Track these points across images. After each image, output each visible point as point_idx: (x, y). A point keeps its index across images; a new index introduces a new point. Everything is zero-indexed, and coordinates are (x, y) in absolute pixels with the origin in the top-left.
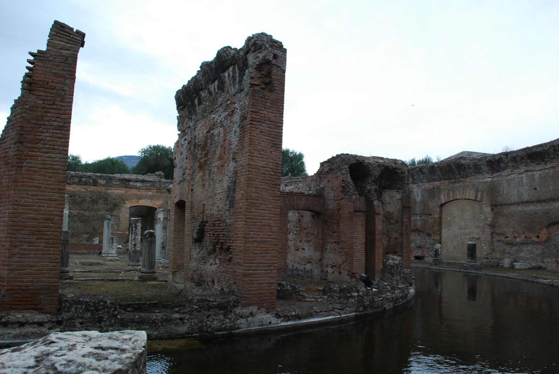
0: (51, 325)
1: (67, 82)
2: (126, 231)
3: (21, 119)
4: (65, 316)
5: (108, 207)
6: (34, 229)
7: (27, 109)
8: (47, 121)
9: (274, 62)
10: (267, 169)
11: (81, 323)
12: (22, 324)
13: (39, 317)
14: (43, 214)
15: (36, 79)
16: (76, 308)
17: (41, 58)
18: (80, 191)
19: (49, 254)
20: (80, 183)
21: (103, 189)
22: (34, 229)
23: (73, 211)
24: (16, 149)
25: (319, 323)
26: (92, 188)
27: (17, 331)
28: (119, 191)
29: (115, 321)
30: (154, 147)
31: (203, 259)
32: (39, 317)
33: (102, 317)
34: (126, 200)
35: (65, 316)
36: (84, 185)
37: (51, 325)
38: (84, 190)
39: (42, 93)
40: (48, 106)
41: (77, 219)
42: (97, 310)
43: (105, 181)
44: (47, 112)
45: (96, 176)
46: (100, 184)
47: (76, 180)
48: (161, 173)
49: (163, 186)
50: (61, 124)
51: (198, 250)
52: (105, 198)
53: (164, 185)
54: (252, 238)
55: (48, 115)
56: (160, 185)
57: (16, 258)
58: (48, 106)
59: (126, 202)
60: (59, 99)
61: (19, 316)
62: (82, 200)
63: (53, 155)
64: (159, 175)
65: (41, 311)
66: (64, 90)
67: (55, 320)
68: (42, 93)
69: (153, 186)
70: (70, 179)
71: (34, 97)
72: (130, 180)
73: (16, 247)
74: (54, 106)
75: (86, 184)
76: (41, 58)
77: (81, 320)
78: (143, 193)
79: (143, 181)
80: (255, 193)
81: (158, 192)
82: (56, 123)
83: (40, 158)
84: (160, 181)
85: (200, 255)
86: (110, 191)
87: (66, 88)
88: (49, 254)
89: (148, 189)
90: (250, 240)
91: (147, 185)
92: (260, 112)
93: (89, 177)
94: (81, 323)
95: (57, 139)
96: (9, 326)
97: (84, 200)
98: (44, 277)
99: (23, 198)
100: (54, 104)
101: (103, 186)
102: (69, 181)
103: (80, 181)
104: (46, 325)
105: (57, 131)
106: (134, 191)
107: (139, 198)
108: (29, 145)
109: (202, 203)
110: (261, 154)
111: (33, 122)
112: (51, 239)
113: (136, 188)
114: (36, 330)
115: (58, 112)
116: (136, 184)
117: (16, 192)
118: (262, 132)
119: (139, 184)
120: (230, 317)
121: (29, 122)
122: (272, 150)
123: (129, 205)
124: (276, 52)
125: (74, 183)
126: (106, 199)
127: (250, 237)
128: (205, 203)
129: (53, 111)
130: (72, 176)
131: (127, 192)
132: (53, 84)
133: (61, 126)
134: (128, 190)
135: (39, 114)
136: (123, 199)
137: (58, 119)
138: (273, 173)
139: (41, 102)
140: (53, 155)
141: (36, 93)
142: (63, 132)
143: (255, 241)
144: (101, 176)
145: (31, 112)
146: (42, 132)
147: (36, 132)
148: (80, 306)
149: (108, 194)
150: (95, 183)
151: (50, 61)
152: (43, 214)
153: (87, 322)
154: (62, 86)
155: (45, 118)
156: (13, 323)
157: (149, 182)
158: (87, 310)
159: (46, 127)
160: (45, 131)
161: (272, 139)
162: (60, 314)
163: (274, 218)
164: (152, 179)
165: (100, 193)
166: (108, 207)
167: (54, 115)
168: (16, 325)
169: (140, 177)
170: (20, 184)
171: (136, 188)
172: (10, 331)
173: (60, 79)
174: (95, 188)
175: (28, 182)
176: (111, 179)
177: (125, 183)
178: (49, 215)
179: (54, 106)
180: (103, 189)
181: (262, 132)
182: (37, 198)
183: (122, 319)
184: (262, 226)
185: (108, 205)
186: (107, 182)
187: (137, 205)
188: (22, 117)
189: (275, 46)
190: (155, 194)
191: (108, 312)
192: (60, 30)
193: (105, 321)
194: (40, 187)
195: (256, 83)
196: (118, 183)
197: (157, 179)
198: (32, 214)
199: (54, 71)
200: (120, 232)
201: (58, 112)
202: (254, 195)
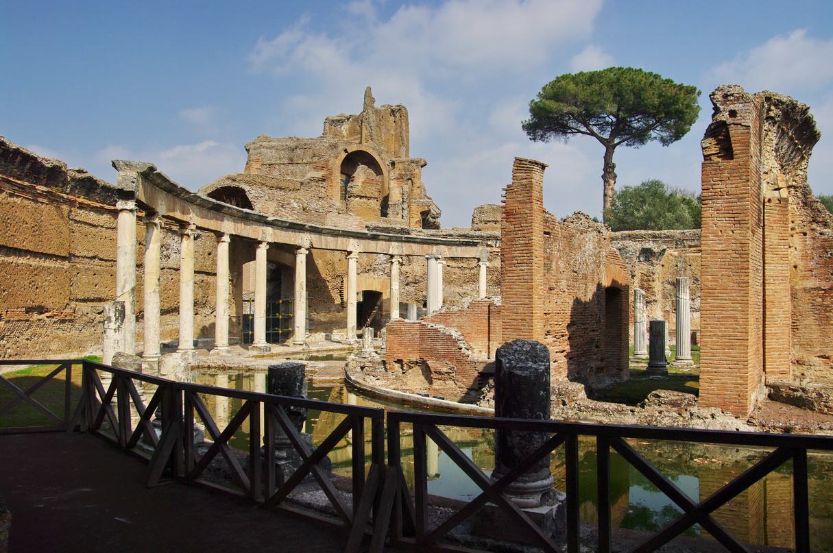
1: (528, 206)
9: (730, 120)
10: (728, 252)
15: (508, 209)
39: (512, 220)
40: (517, 229)
54: (710, 332)
55: (517, 236)
66: (526, 214)
68: (512, 220)
80: (711, 281)
87: (527, 211)
90: (709, 334)
92: (714, 187)
110: (718, 236)
115: (523, 232)
118: (718, 210)
120: (684, 415)
122: (734, 229)
124: (732, 107)
127: (707, 331)
135: (512, 236)
138: (738, 256)
143: (715, 335)
146: (515, 251)
154: (524, 210)
160: (517, 249)
161: (733, 216)
163: (740, 308)
181: (718, 210)
184: (722, 317)
189: (731, 101)
191: (568, 397)
192: (518, 167)
195: (714, 152)
202: (709, 284)
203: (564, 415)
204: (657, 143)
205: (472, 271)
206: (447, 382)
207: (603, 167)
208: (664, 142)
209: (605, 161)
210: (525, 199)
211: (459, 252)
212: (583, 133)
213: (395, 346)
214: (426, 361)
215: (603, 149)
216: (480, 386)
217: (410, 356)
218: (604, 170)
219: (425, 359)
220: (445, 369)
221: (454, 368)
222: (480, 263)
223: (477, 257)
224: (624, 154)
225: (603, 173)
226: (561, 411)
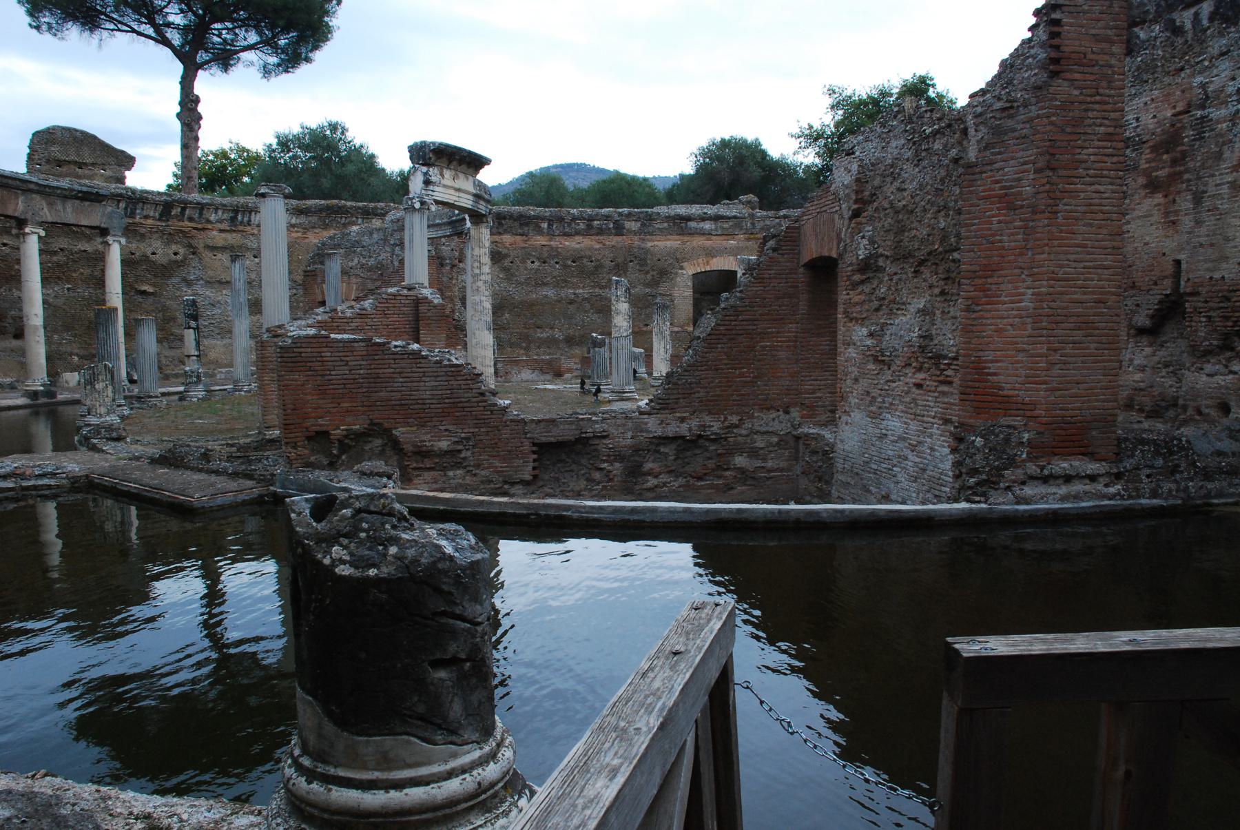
0: (1107, 480)
2: (688, 325)
3: (1049, 128)
4: (1128, 464)
5: (649, 277)
6: (1081, 319)
7: (1057, 107)
8: (1090, 126)
11: (1148, 476)
12: (1068, 479)
13: (1092, 467)
14: (1093, 293)
16: (1142, 451)
17: (1072, 9)
18: (591, 249)
19: (1103, 361)
20: (589, 231)
21: (636, 241)
22: (1081, 319)
23: (581, 291)
24: (1045, 180)
25: (1031, 516)
26: (614, 240)
27: (1063, 490)
28: (668, 243)
29: (1196, 473)
30: (723, 141)
31: (1166, 366)
32: (1092, 467)
33: (1178, 466)
34: (684, 259)
35: (1128, 464)
36: (597, 234)
37: (1107, 480)
38: (597, 246)
39: (1077, 76)
40: (1089, 99)
41: (588, 306)
42: (1171, 453)
43: (639, 224)
44: (1086, 110)
45: (620, 214)
46: (630, 231)
47: (582, 226)
48: (751, 197)
49: (759, 226)
50: (1111, 130)
51: (1148, 350)
52: (641, 259)
53: (762, 224)
55: (1090, 114)
56: (753, 224)
57: (1056, 371)
58: (1089, 99)
59: (685, 264)
60: (1104, 84)
61: (1065, 465)
62: (596, 268)
63: (1102, 188)
64: (749, 202)
65: (1093, 456)
66: (1111, 66)
67: (1115, 470)
68: (1077, 76)
69: (738, 226)
70: (569, 224)
71: (1066, 84)
72: (688, 219)
73: (1055, 351)
74: (1098, 98)
75: (601, 232)
76: (1072, 9)
77: (1148, 471)
78: (717, 242)
79: (717, 218)
81: (748, 240)
82: (1102, 129)
83: (1082, 195)
84: (752, 216)
85: (1156, 359)
86: (649, 244)
87: (1113, 61)
88: (1103, 361)
89: (728, 235)
91: (726, 226)
93: (607, 217)
94: (1148, 476)
95: (1106, 159)
96: (1052, 482)
97: (599, 267)
98: (1098, 401)
99: (1062, 266)
100: (1098, 94)
101: (635, 233)
102: (567, 230)
103: (590, 227)
104: (1101, 480)
105: (1105, 144)
106: (698, 241)
107: (711, 254)
108: (1065, 173)
109: (1170, 259)
111: (1068, 130)
112: (1107, 335)
113: (703, 233)
114: (1087, 488)
115: (1105, 107)
116: (701, 225)
117: (1052, 257)
119: (707, 226)
121: (1063, 131)
123: (690, 270)
125: (578, 233)
126: (642, 262)
128: (1182, 257)
129: (1097, 106)
130: (574, 219)
131: (684, 243)
132: (1090, 56)
133: (1110, 134)
134: (686, 238)
135: (1077, 113)
136: (678, 259)
137: (1106, 122)
139: (1076, 92)
140: (1102, 188)
141: (1068, 75)
142: (1115, 144)
144: (630, 214)
145: (1064, 114)
146: (1083, 148)
147: (1075, 147)
148: (1146, 448)
149: (647, 251)
150: (619, 230)
151: (1085, 12)
152: (1093, 293)
153: (1158, 474)
154: (1106, 57)
155: (1087, 122)
156: (1056, 477)
157: (729, 218)
158: (1157, 453)
159: (1088, 137)
162: (1121, 461)
164: (734, 212)
165: (630, 248)
166: (649, 277)
167: (1099, 115)
168: (1060, 481)
169: (711, 210)
170: (1056, 243)
171: (703, 233)
172: (1054, 490)
173: (1104, 45)
174: (619, 239)
175: (1067, 238)
176: (650, 218)
177: (680, 224)
178: (1101, 293)
179: (1098, 98)
180: (636, 241)
182: (1082, 265)
183: (1205, 468)
185: (647, 273)
186: (643, 225)
187: (708, 268)
188: (1052, 123)
190: (742, 244)
193: (1182, 472)
194: (1085, 246)
196: (666, 225)
197: (746, 211)
198: (1076, 293)
199: (1093, 32)
200: (676, 329)
201: (1105, 107)
203: (1182, 494)
204: (255, 74)
205: (55, 258)
206: (451, 474)
207: (178, 99)
208: (267, 71)
209: (182, 89)
210: (1109, 32)
211: (69, 213)
212: (139, 34)
213: (309, 397)
214: (390, 430)
215: (178, 68)
216: (537, 472)
217: (349, 419)
218: (180, 104)
219: (386, 425)
220: (444, 444)
221: (468, 439)
222: (110, 239)
223: (103, 225)
224: (205, 84)
225: (178, 109)
226: (1173, 486)
